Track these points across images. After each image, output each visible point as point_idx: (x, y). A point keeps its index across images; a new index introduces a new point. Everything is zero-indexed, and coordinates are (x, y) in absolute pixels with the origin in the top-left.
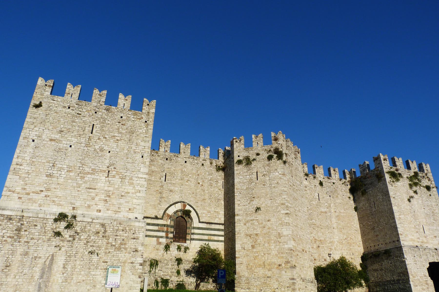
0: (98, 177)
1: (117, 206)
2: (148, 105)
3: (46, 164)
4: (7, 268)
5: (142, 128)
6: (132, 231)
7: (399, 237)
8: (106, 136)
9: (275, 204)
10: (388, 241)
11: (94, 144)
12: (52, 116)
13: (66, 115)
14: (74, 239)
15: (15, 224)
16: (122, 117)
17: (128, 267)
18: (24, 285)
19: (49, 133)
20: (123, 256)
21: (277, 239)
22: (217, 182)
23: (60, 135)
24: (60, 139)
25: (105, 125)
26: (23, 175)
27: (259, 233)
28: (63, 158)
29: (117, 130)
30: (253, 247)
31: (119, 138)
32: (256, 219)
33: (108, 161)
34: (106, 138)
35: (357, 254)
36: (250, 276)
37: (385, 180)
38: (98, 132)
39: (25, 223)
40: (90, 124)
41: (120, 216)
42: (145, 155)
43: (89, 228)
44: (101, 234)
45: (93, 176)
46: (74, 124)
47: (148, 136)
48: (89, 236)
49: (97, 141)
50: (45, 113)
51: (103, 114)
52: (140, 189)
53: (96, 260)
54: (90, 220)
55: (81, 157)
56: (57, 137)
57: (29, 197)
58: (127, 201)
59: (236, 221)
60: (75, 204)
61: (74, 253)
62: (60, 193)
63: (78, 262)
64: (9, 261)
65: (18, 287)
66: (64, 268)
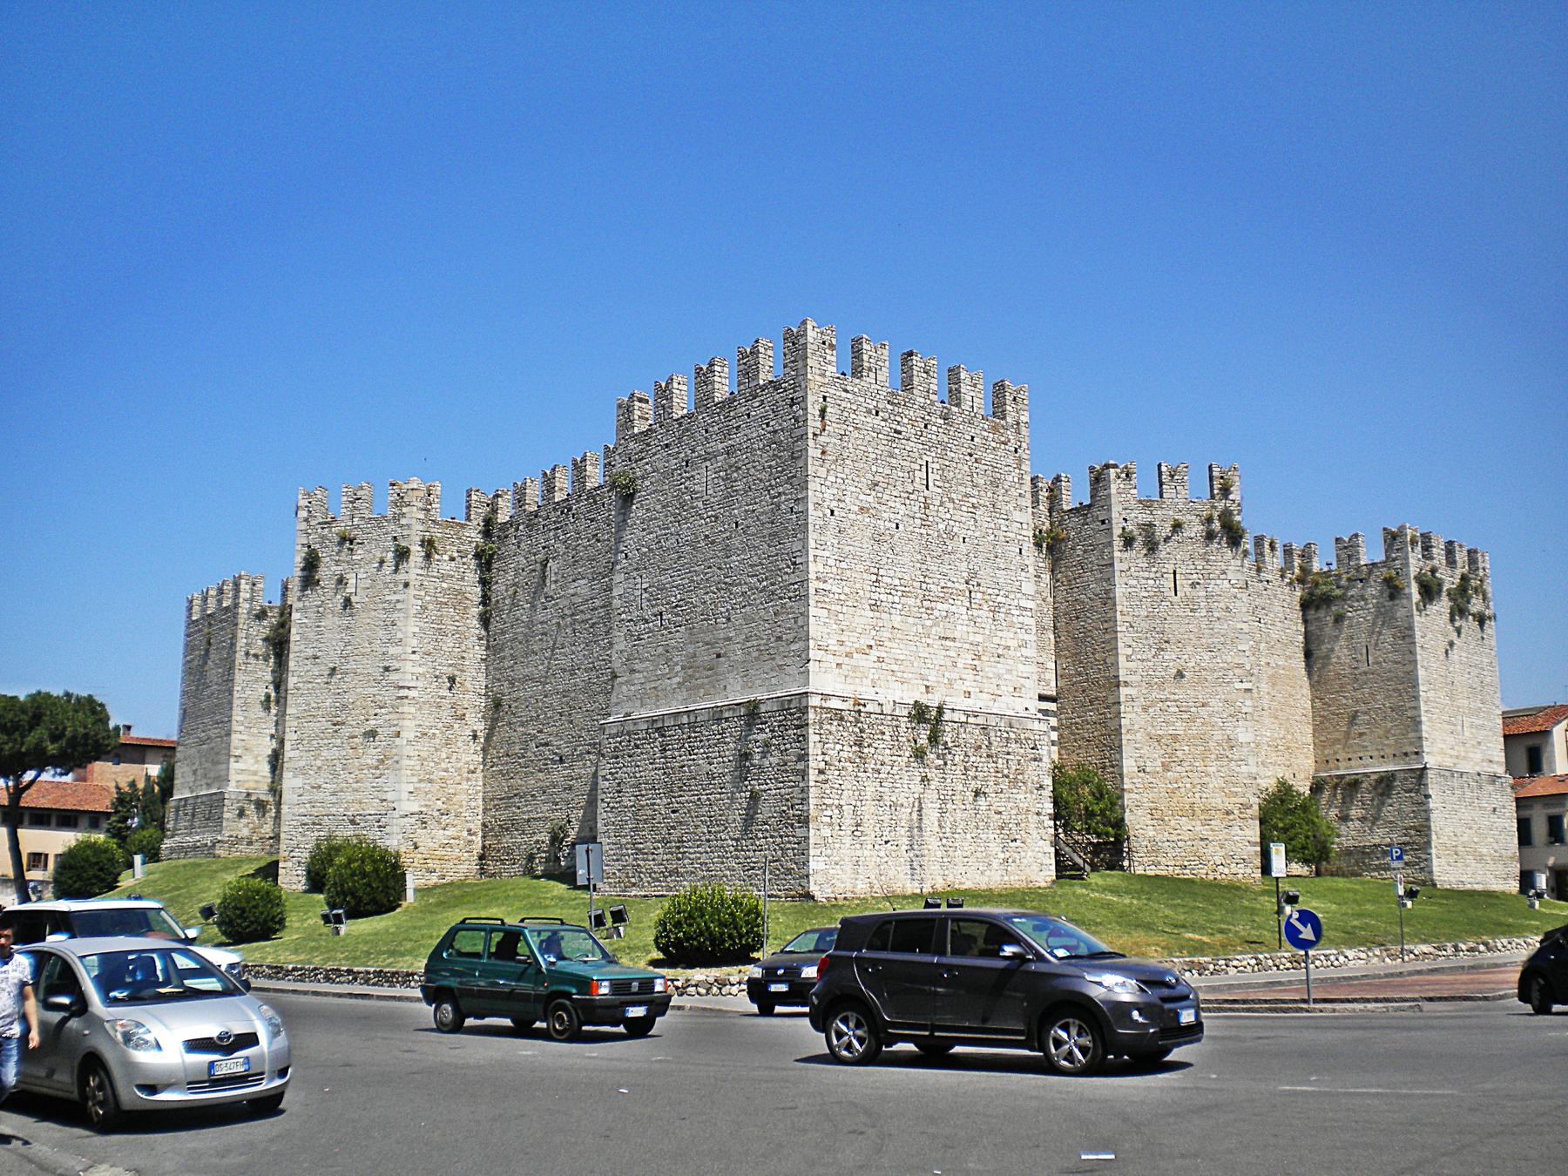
0: (953, 609)
1: (994, 681)
2: (1015, 399)
3: (865, 576)
4: (859, 828)
5: (1011, 469)
6: (1029, 742)
7: (1422, 746)
8: (954, 496)
9: (1221, 665)
10: (1389, 751)
11: (936, 519)
12: (852, 441)
13: (875, 435)
14: (946, 764)
15: (851, 729)
16: (973, 438)
17: (1033, 819)
18: (889, 863)
19: (854, 489)
20: (1024, 798)
21: (1224, 750)
22: (1039, 577)
23: (873, 493)
24: (877, 506)
25: (947, 463)
26: (833, 607)
27: (1182, 732)
28: (890, 561)
29: (969, 478)
30: (1166, 767)
31: (974, 501)
32: (1172, 697)
33: (966, 564)
34: (952, 500)
35: (1303, 776)
36: (1160, 836)
37: (1409, 597)
38: (937, 483)
39: (866, 726)
40: (919, 461)
41: (1004, 706)
42: (1024, 549)
43: (964, 736)
44: (984, 751)
45: (946, 606)
46: (894, 461)
47: (1022, 492)
48: (966, 755)
49: (941, 509)
50: (836, 430)
51: (940, 430)
52: (1027, 637)
53: (984, 808)
54: (963, 719)
55: (919, 557)
56: (870, 499)
57: (853, 662)
58: (1009, 668)
59: (1122, 699)
60: (929, 678)
61: (950, 793)
62: (899, 651)
63: (959, 814)
64: (859, 813)
65: (882, 867)
66: (940, 826)
